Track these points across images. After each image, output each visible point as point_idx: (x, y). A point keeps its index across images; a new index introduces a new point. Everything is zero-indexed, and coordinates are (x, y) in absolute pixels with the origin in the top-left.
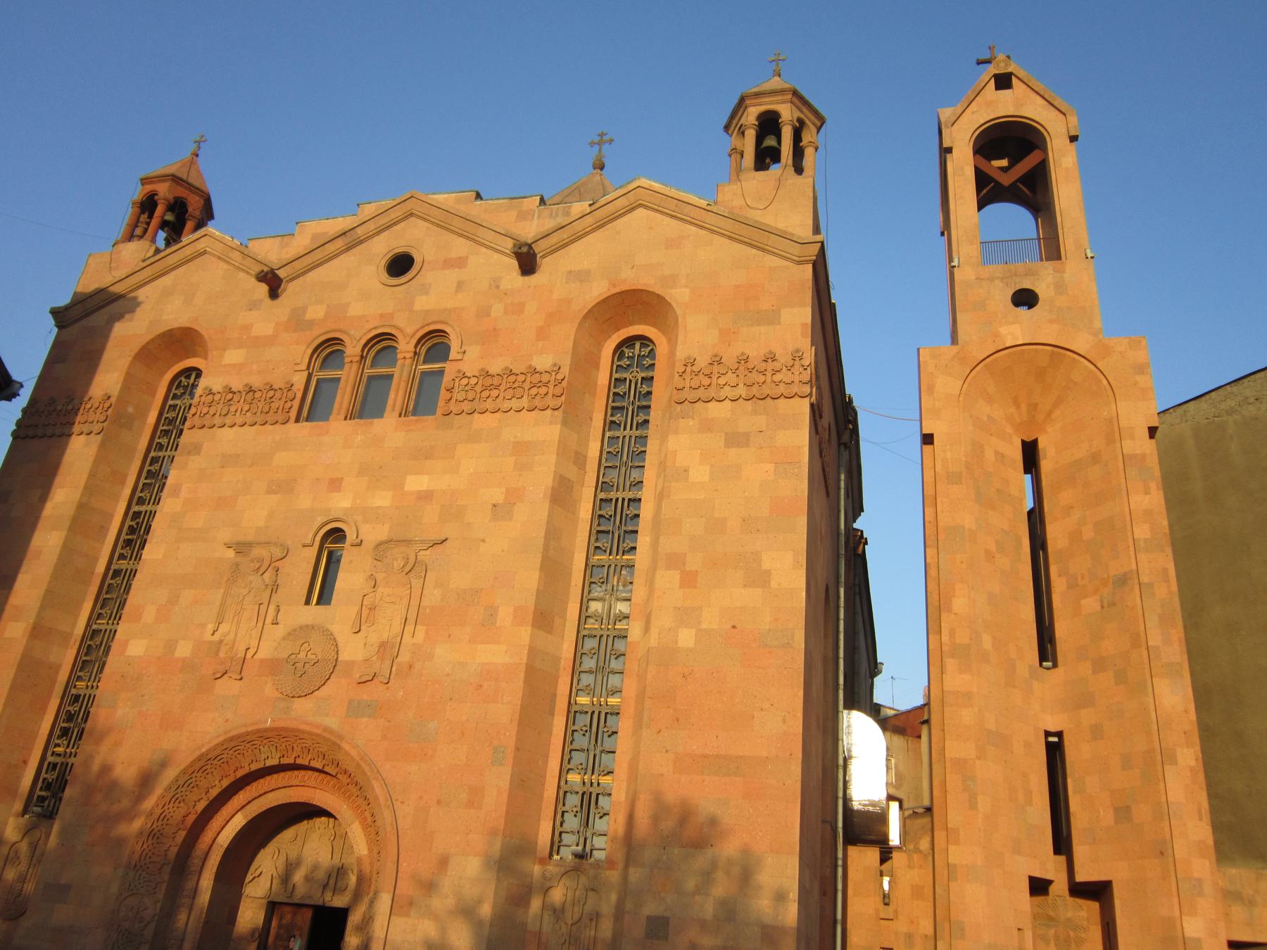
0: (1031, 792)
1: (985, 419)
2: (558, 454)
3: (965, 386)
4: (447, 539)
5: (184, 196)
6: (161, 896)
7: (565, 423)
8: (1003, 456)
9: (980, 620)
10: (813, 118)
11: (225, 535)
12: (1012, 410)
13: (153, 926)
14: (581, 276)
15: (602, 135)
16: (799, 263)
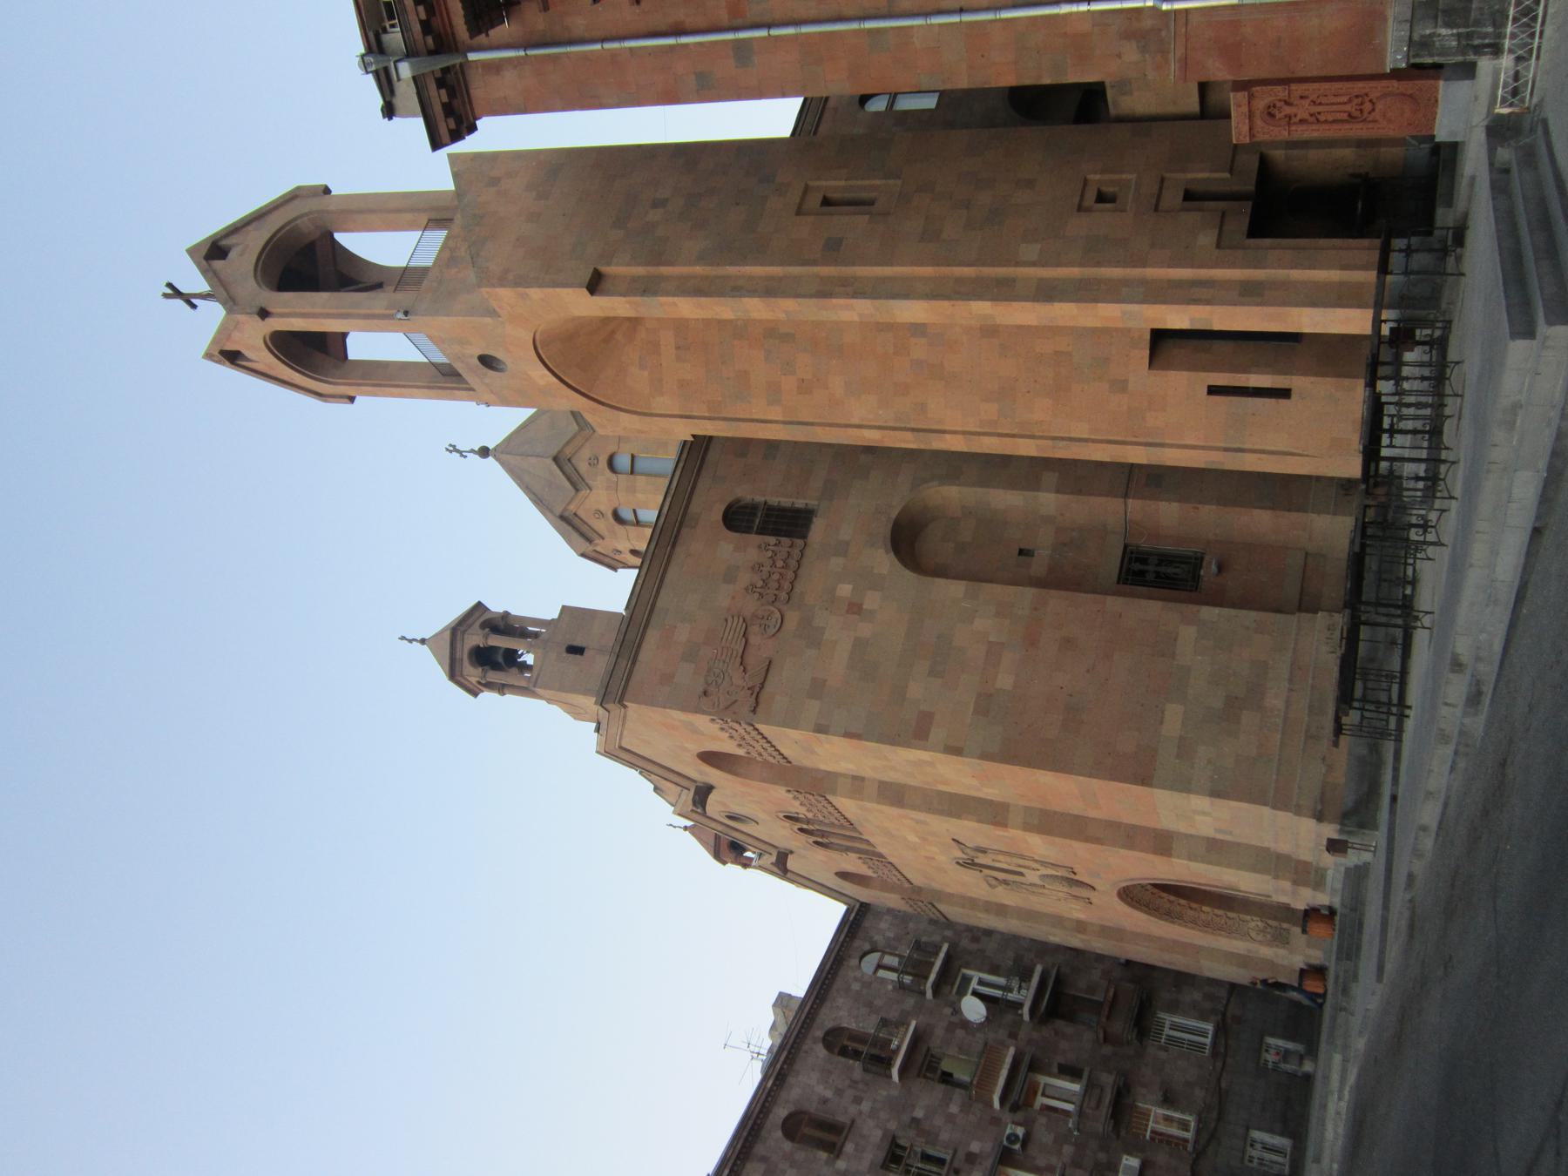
0: (1056, 353)
1: (646, 373)
2: (862, 800)
3: (623, 407)
4: (954, 840)
5: (726, 846)
6: (1248, 918)
7: (834, 793)
8: (678, 348)
9: (881, 412)
10: (459, 646)
11: (988, 888)
12: (619, 336)
13: (1270, 922)
14: (701, 773)
15: (451, 451)
16: (625, 707)
